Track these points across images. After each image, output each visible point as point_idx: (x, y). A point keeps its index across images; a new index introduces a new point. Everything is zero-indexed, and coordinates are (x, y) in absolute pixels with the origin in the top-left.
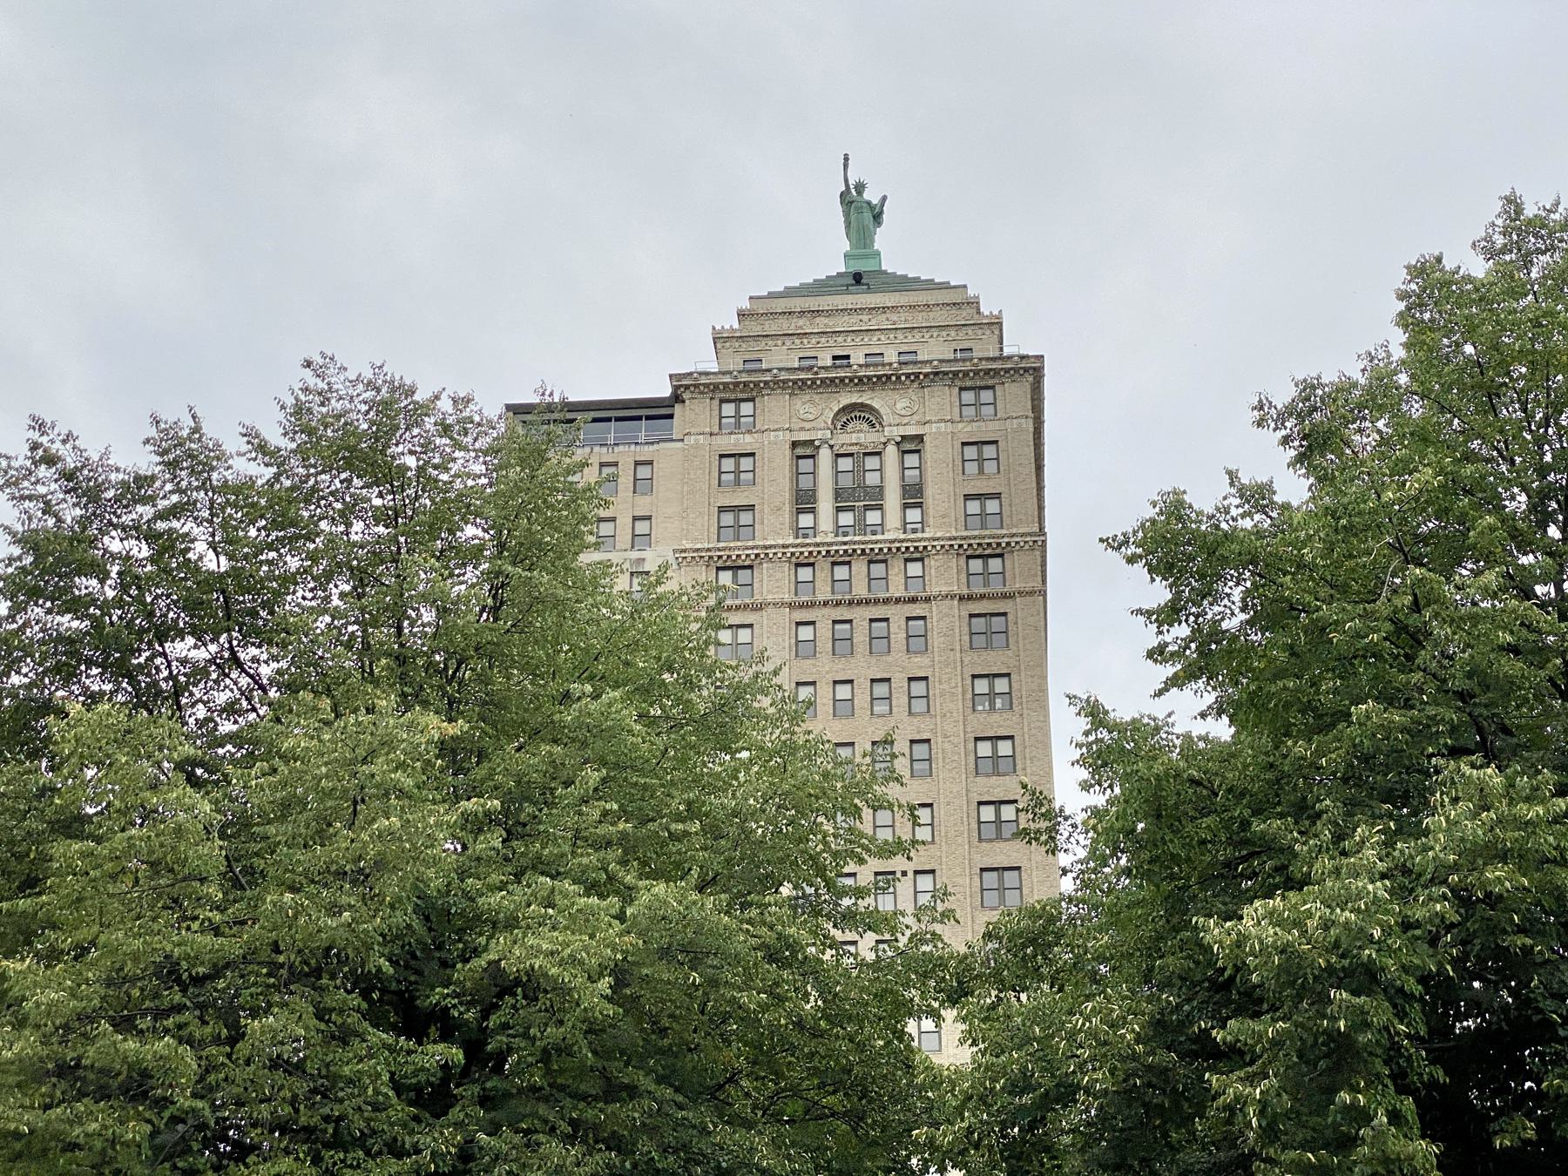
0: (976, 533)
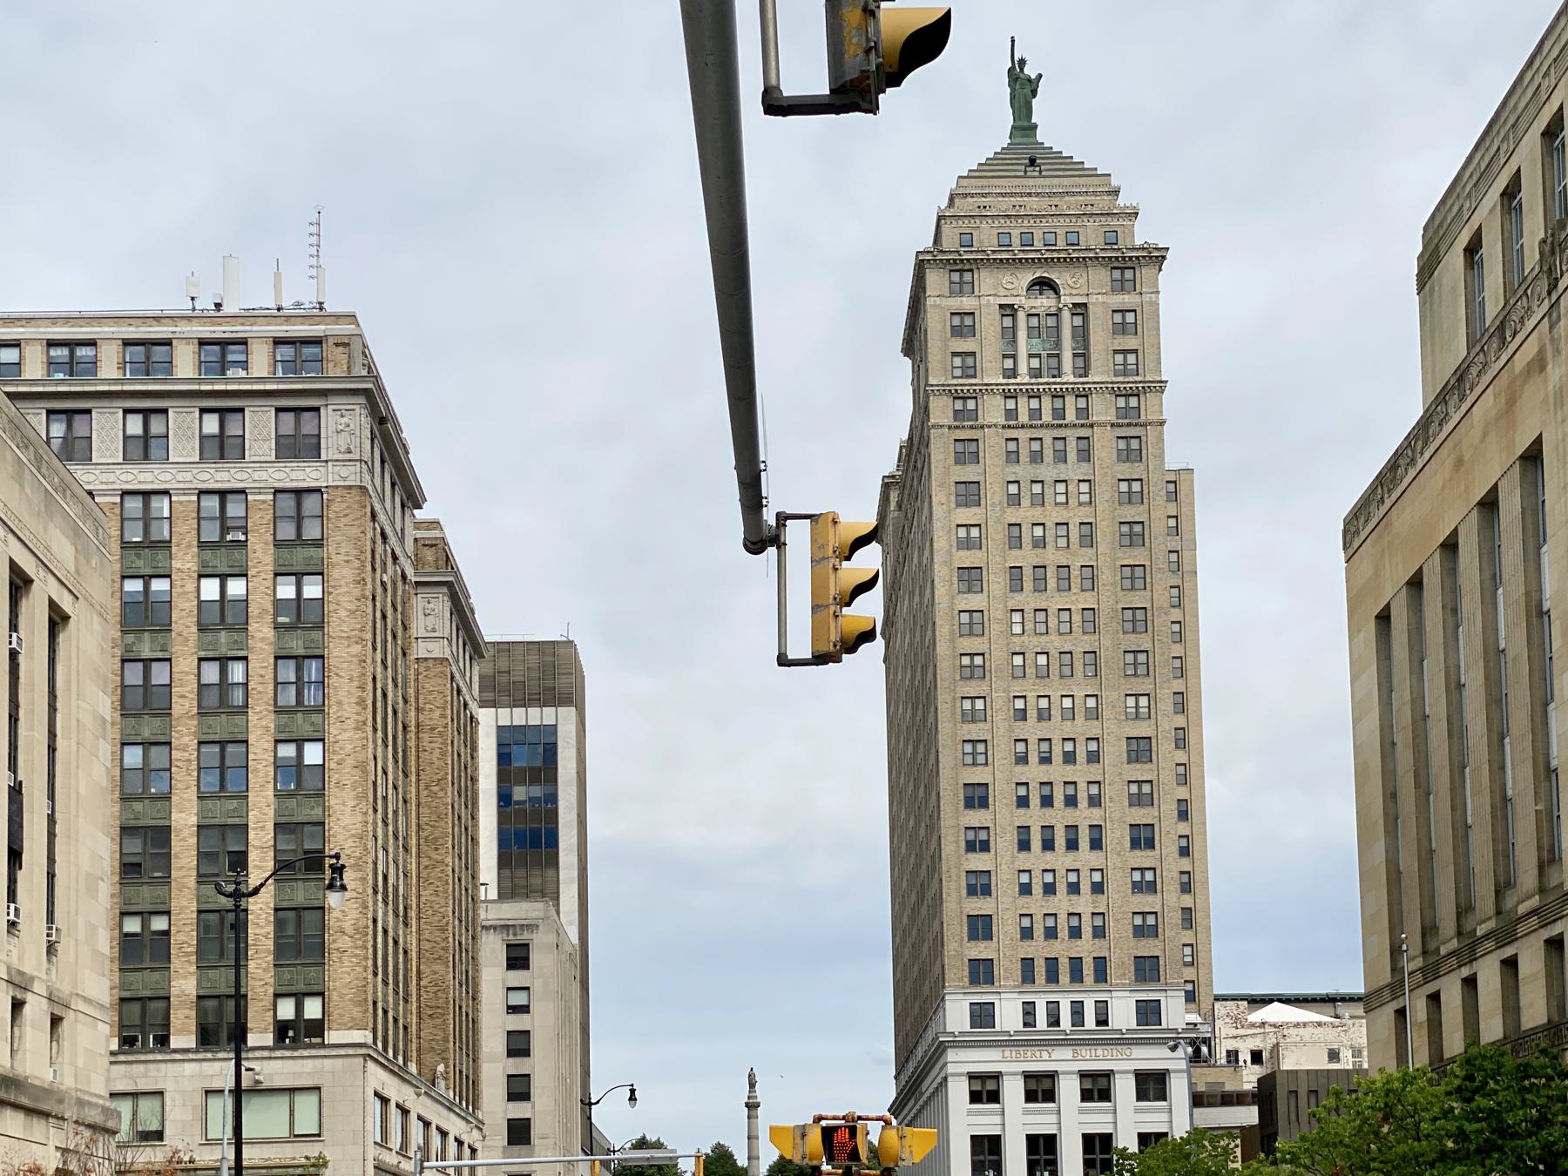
0: (1121, 379)
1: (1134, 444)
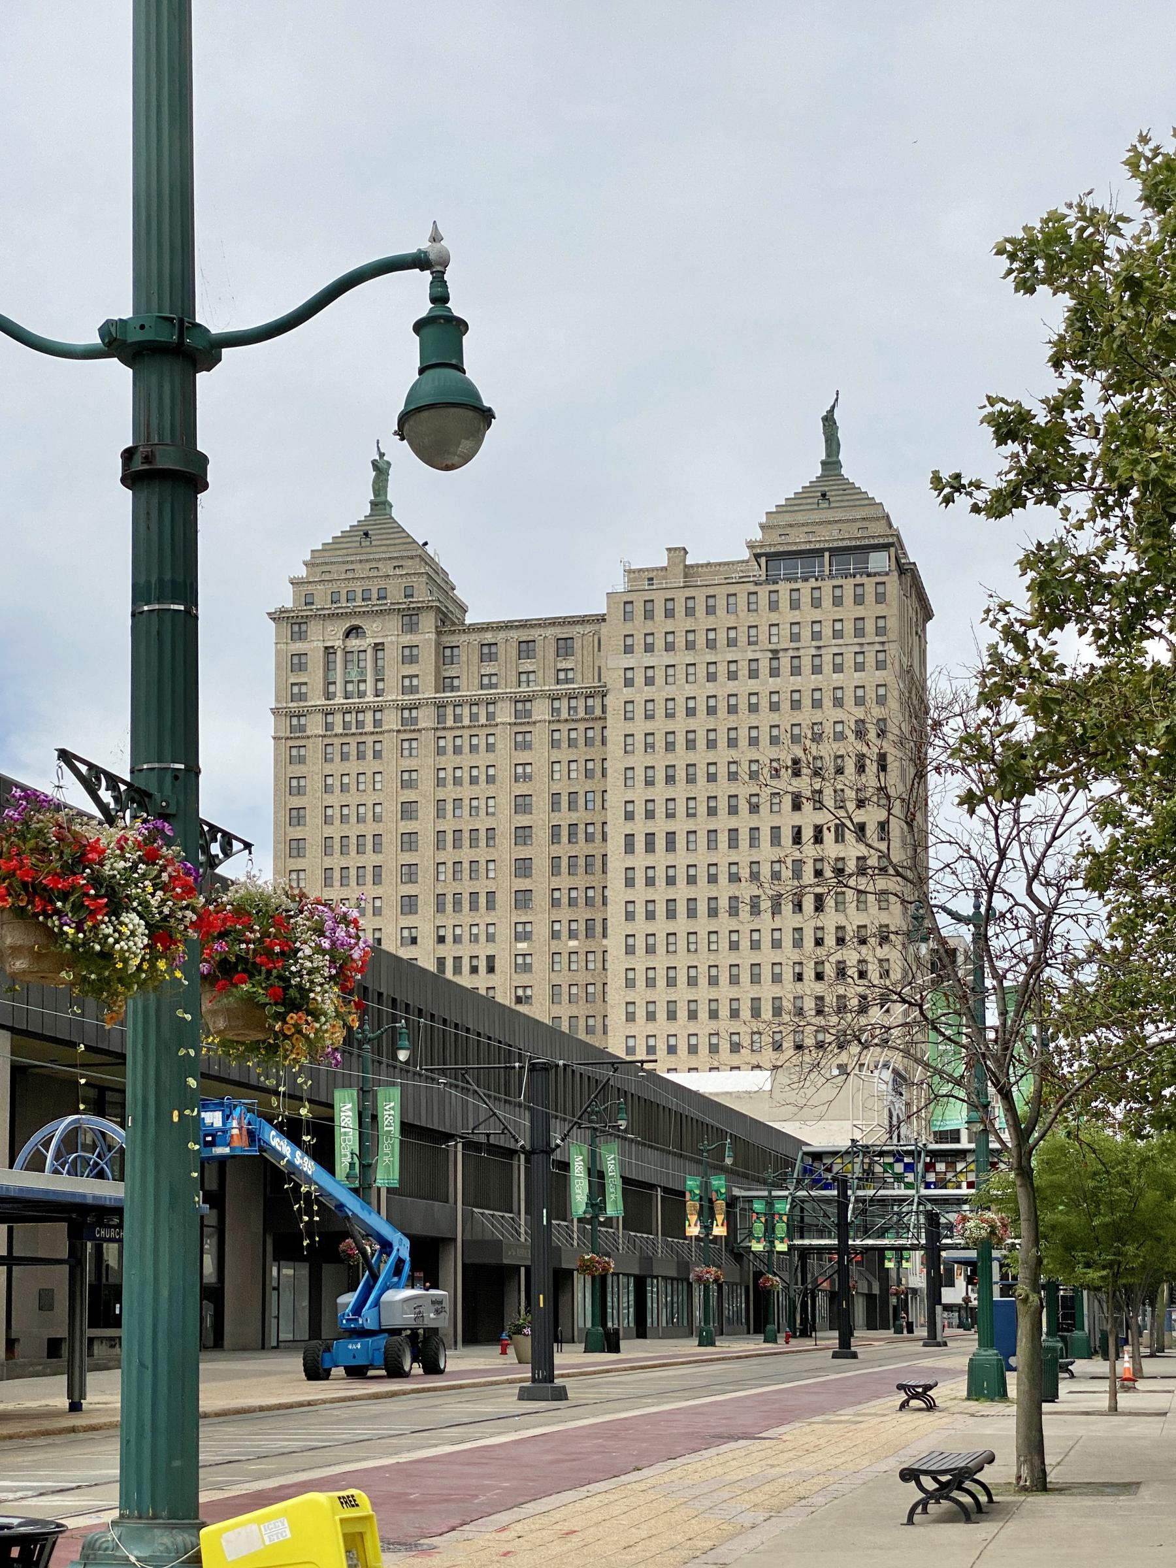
1: (414, 744)
